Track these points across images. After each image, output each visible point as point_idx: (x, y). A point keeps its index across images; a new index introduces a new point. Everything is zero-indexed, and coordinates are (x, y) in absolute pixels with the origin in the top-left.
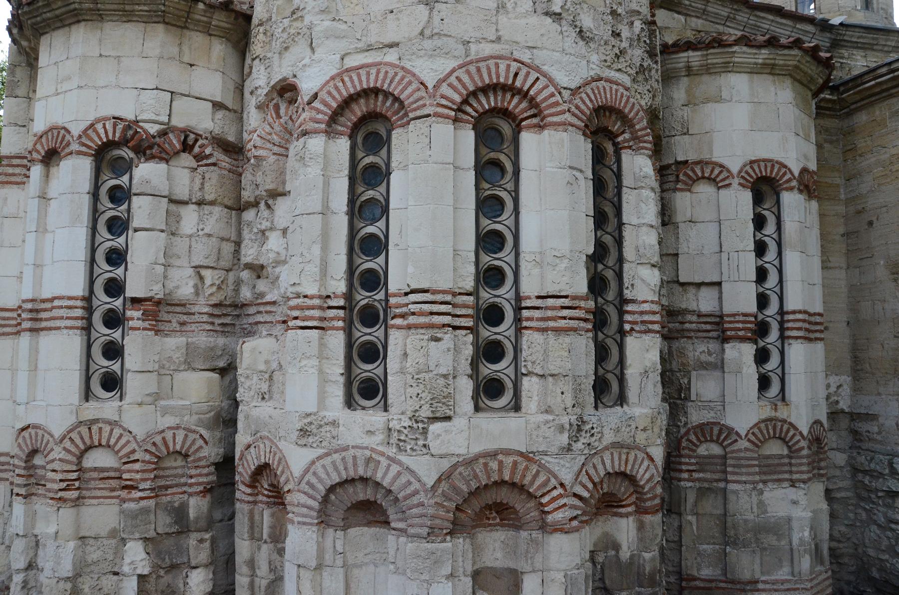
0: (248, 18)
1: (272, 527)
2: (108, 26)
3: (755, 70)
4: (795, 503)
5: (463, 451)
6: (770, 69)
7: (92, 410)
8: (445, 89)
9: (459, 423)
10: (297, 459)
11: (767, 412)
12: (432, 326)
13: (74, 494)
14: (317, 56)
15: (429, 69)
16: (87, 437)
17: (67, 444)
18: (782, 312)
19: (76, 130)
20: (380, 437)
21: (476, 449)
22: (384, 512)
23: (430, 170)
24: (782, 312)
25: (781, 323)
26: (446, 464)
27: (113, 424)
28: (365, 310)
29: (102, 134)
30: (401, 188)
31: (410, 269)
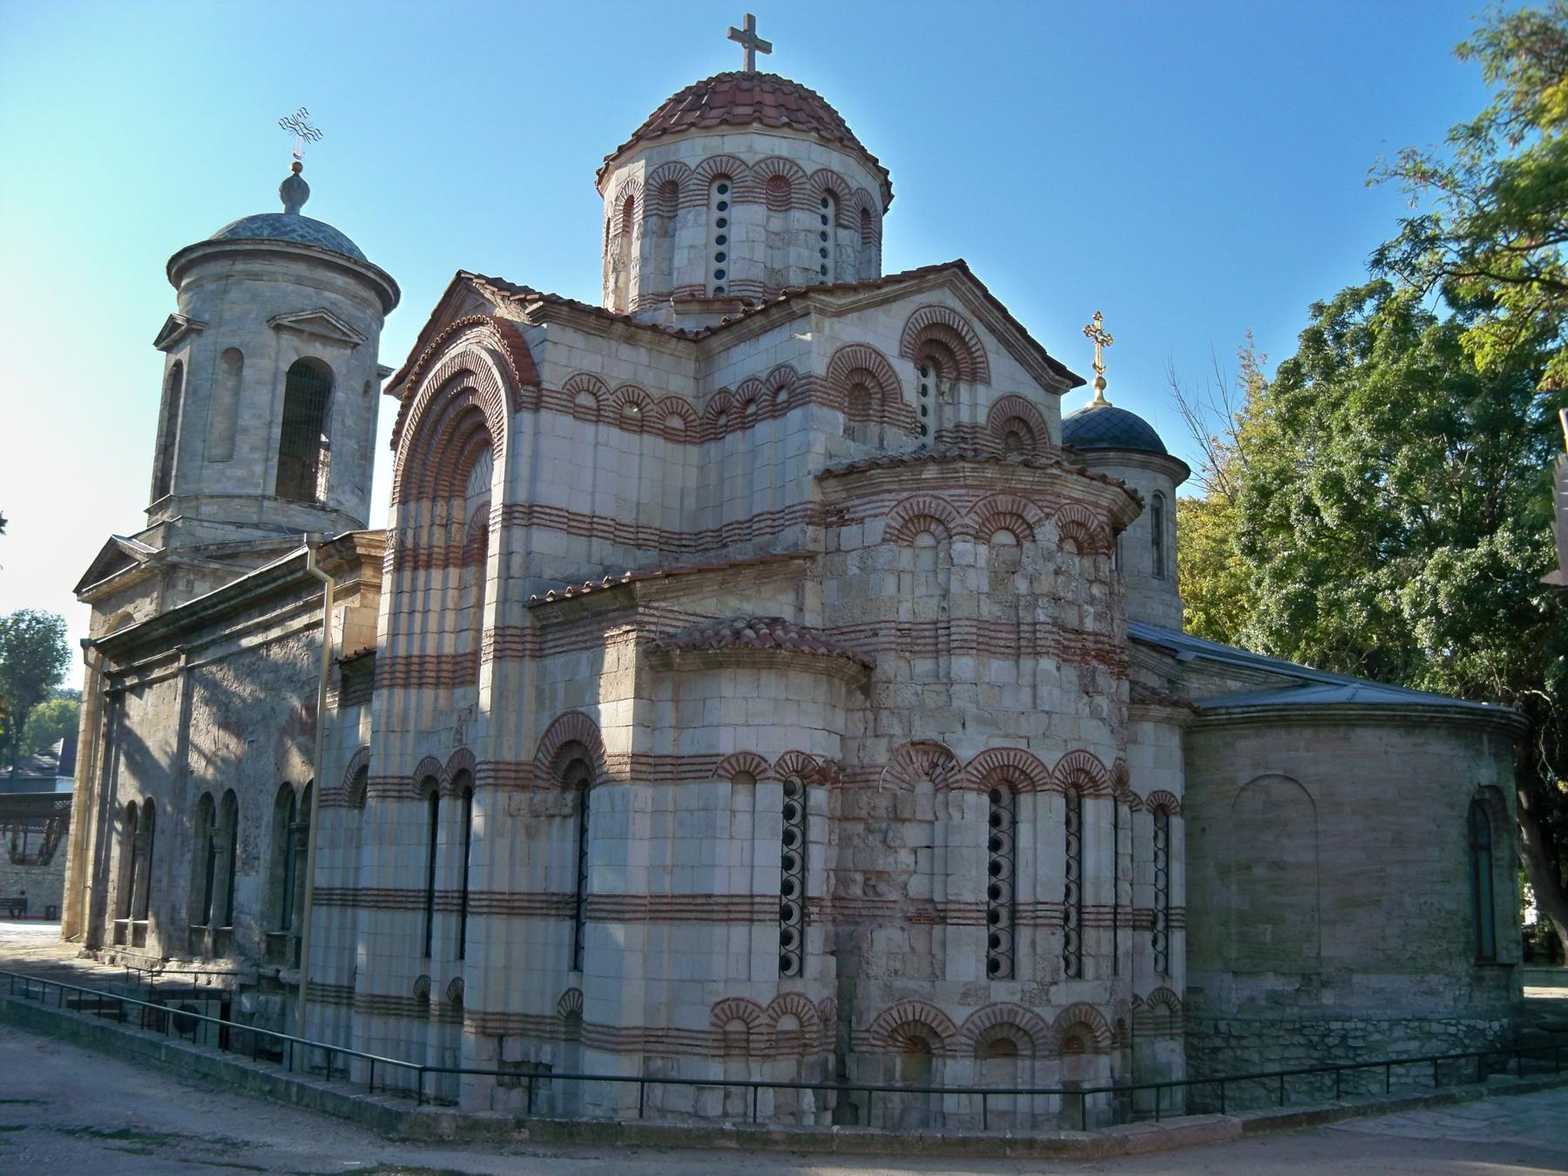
0: (867, 668)
1: (903, 1070)
2: (791, 673)
3: (1158, 721)
4: (1173, 1051)
5: (1064, 1002)
6: (1168, 720)
7: (789, 986)
8: (1057, 774)
9: (1062, 985)
10: (960, 1015)
11: (1159, 983)
12: (1051, 925)
13: (772, 1052)
15: (1051, 758)
16: (782, 1005)
17: (771, 1012)
18: (1167, 907)
19: (773, 761)
20: (1019, 996)
21: (1072, 1000)
22: (1015, 1045)
23: (1041, 819)
24: (1167, 907)
25: (1167, 915)
26: (1058, 1011)
27: (799, 995)
28: (1001, 913)
31: (1039, 889)
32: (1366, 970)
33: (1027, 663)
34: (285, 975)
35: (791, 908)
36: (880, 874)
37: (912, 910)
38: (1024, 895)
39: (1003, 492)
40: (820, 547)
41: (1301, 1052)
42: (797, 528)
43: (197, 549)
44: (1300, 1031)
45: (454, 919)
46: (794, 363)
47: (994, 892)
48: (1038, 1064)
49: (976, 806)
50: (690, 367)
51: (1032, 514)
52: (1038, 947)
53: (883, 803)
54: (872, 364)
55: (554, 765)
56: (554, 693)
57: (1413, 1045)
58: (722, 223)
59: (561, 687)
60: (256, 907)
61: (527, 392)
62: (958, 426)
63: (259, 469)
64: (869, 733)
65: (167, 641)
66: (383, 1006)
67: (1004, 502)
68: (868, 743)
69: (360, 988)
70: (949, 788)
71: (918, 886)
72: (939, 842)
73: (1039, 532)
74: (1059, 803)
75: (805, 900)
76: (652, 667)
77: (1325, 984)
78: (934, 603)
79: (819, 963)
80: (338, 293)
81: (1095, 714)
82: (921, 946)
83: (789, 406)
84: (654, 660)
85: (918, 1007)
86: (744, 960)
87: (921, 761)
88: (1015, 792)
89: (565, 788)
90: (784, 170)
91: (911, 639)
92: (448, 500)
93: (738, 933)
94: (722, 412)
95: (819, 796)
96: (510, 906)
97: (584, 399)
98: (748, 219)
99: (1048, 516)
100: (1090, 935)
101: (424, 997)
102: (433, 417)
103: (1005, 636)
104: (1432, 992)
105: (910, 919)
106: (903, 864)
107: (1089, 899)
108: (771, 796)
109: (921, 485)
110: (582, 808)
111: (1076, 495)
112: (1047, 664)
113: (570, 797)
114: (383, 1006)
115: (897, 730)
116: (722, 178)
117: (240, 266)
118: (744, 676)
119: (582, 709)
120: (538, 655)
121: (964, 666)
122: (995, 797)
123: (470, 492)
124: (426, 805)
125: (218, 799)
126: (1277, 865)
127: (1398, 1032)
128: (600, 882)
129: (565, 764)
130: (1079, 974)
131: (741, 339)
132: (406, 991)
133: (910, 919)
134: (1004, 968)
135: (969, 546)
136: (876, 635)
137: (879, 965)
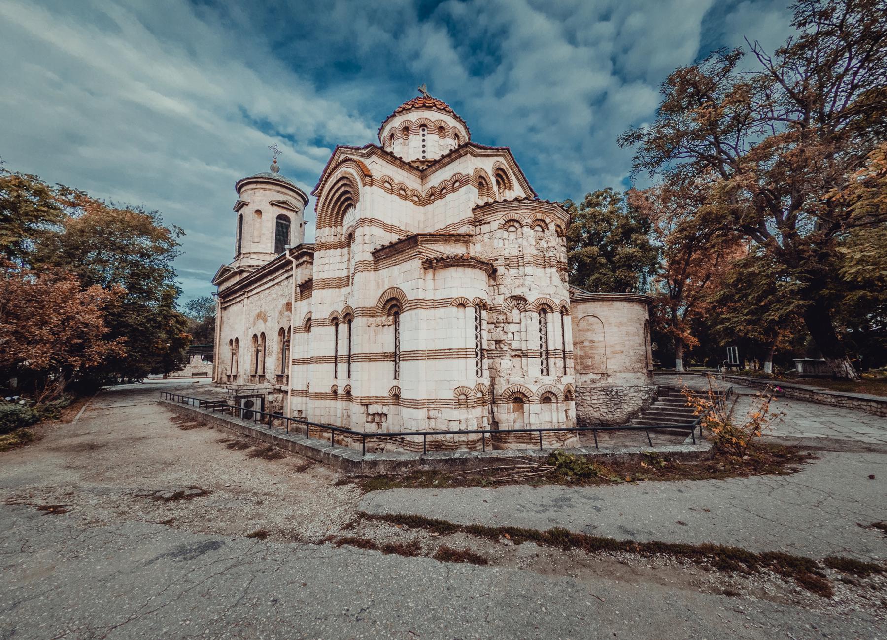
0: (495, 271)
10: (534, 389)
14: (532, 292)
15: (557, 302)
22: (550, 399)
29: (477, 301)
32: (620, 372)
33: (548, 270)
34: (284, 388)
35: (482, 353)
37: (513, 353)
38: (551, 347)
40: (473, 233)
41: (603, 397)
43: (250, 266)
44: (603, 390)
45: (346, 365)
47: (541, 346)
48: (559, 405)
49: (535, 315)
50: (419, 181)
51: (548, 220)
52: (556, 364)
53: (502, 317)
54: (485, 176)
55: (384, 307)
56: (383, 282)
57: (636, 394)
58: (424, 141)
59: (386, 280)
60: (273, 367)
61: (368, 179)
63: (269, 245)
66: (320, 396)
67: (539, 216)
69: (311, 390)
70: (526, 311)
71: (515, 345)
74: (560, 315)
75: (482, 350)
76: (425, 268)
77: (608, 376)
78: (517, 249)
79: (486, 373)
82: (518, 365)
83: (460, 187)
84: (426, 266)
86: (465, 374)
87: (515, 302)
88: (545, 312)
89: (389, 315)
90: (443, 125)
91: (509, 263)
92: (336, 226)
93: (463, 361)
94: (432, 194)
96: (369, 358)
98: (433, 139)
100: (567, 360)
101: (335, 392)
102: (330, 197)
103: (540, 261)
104: (638, 378)
107: (567, 349)
108: (470, 312)
109: (512, 209)
110: (396, 322)
112: (554, 270)
113: (391, 318)
114: (320, 396)
115: (507, 292)
116: (423, 126)
117: (259, 186)
118: (460, 269)
120: (375, 270)
121: (529, 270)
122: (539, 314)
123: (345, 222)
124: (333, 328)
125: (259, 336)
127: (632, 390)
128: (404, 347)
129: (388, 307)
130: (565, 374)
131: (440, 168)
132: (328, 390)
134: (545, 373)
135: (529, 229)
136: (497, 260)
137: (504, 373)
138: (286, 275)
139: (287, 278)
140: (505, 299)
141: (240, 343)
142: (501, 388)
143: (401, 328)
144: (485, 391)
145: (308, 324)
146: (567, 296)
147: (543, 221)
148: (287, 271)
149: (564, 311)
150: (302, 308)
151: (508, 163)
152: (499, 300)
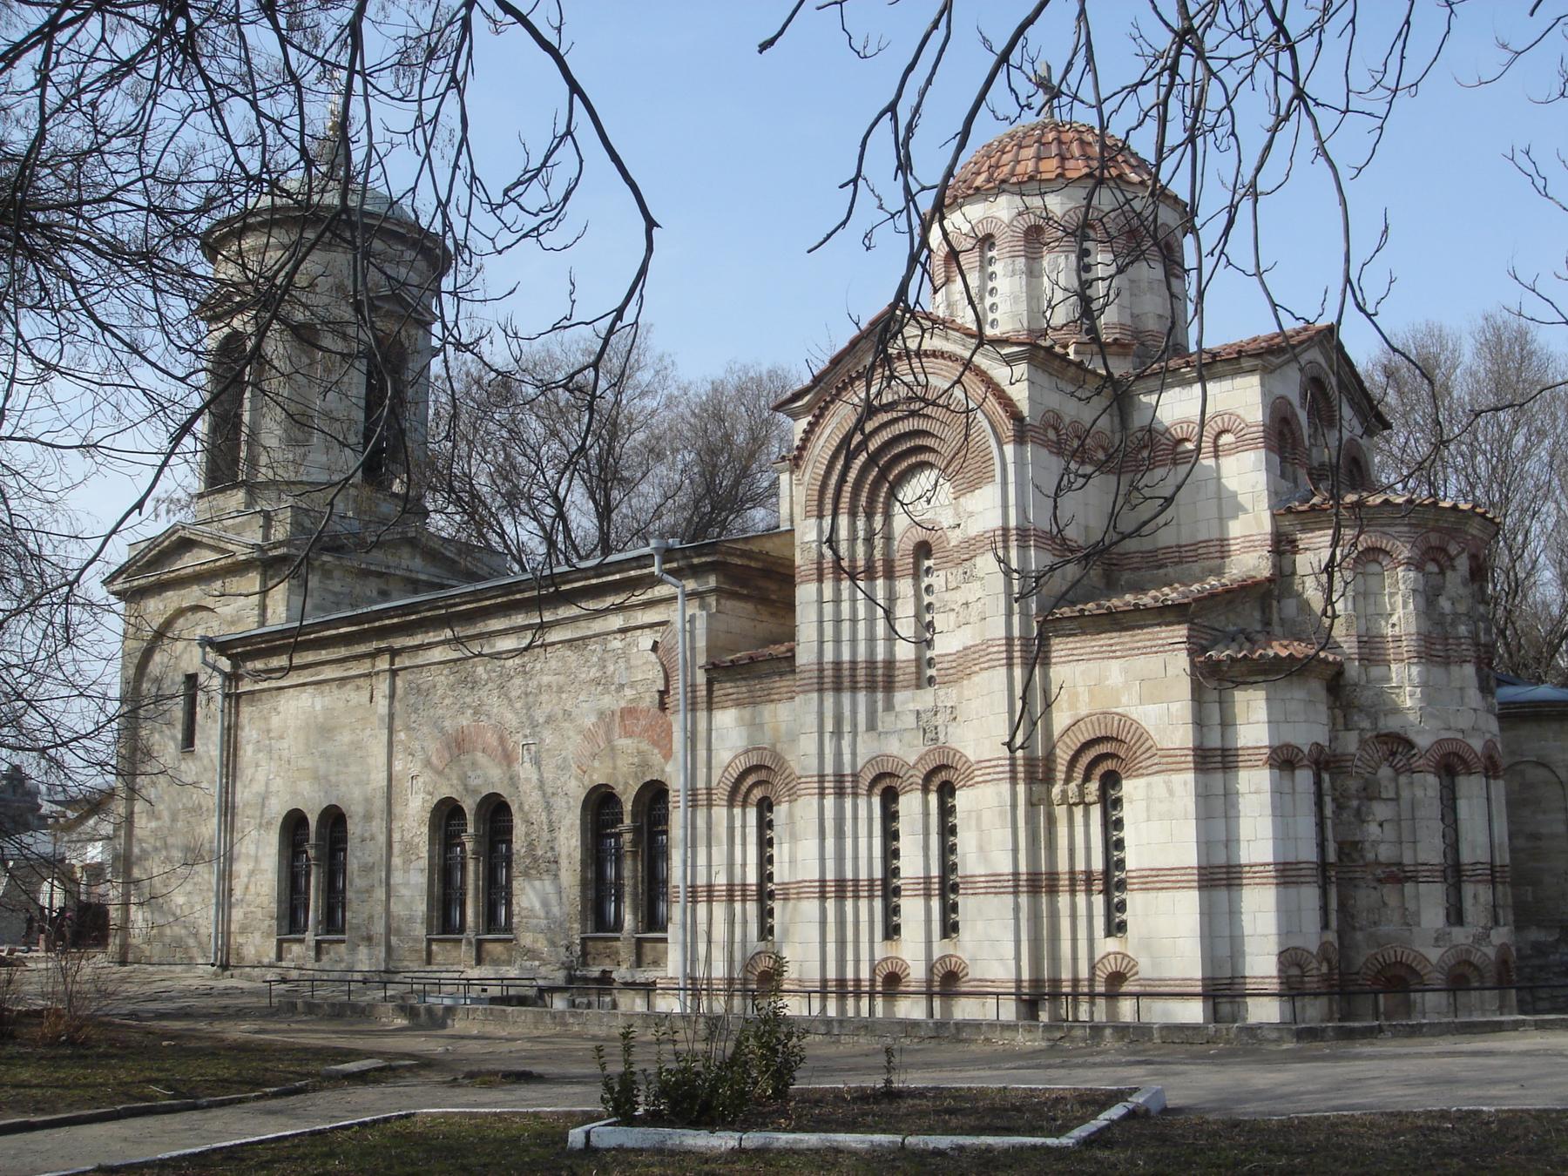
10: (1434, 955)
15: (1477, 744)
28: (1454, 873)
30: (1462, 805)
33: (1454, 669)
36: (1355, 844)
38: (1466, 857)
39: (1433, 530)
42: (1256, 555)
46: (1241, 412)
51: (1453, 549)
52: (1476, 897)
53: (1353, 785)
62: (1322, 465)
64: (1340, 726)
65: (347, 640)
67: (1434, 539)
68: (1341, 734)
71: (1385, 853)
72: (1406, 814)
73: (1457, 562)
80: (409, 271)
81: (1490, 710)
83: (1235, 449)
85: (1399, 950)
95: (1326, 777)
97: (1052, 435)
99: (1463, 550)
105: (1379, 881)
106: (1379, 837)
111: (1475, 532)
113: (1093, 787)
115: (1366, 724)
119: (1119, 710)
125: (469, 805)
126: (1535, 837)
128: (1133, 858)
133: (1379, 881)
138: (616, 621)
139: (623, 631)
140: (1363, 743)
141: (354, 828)
142: (1363, 956)
143: (1129, 813)
144: (1335, 958)
145: (758, 786)
146: (1493, 725)
147: (1443, 550)
148: (619, 608)
149: (1491, 769)
150: (728, 733)
151: (1328, 359)
152: (1350, 743)
